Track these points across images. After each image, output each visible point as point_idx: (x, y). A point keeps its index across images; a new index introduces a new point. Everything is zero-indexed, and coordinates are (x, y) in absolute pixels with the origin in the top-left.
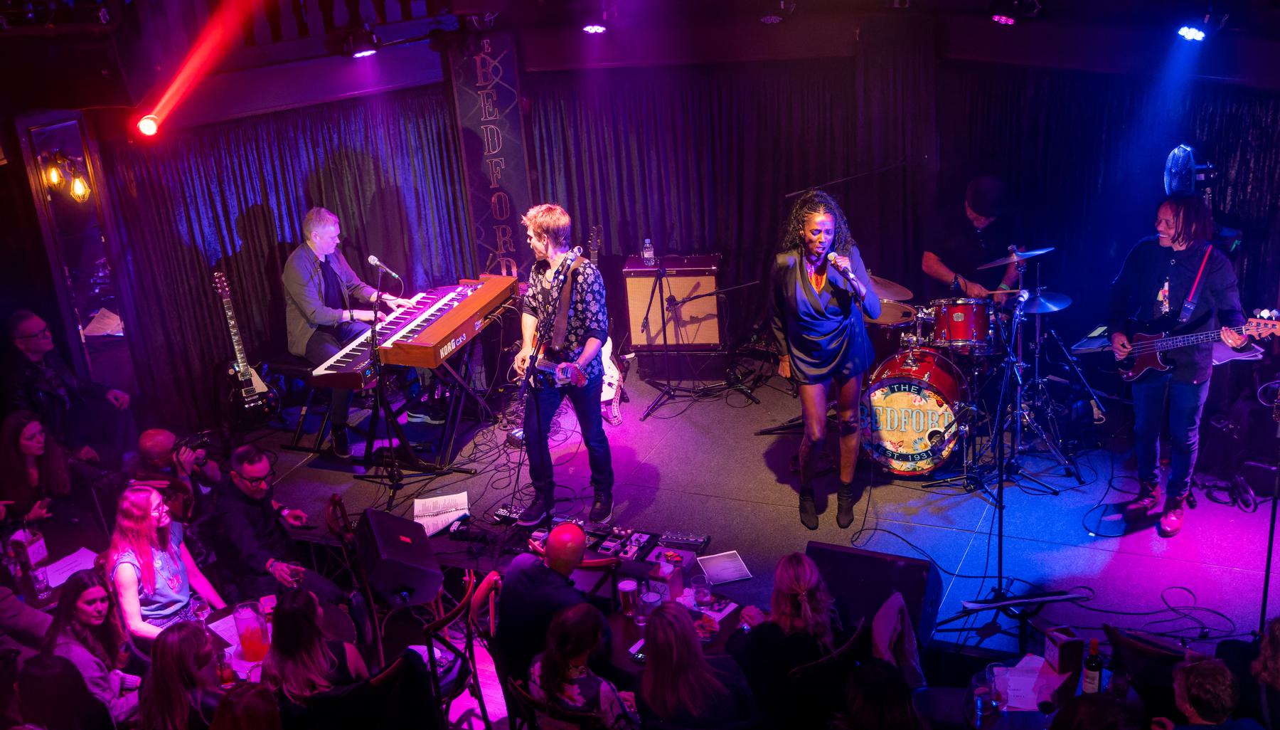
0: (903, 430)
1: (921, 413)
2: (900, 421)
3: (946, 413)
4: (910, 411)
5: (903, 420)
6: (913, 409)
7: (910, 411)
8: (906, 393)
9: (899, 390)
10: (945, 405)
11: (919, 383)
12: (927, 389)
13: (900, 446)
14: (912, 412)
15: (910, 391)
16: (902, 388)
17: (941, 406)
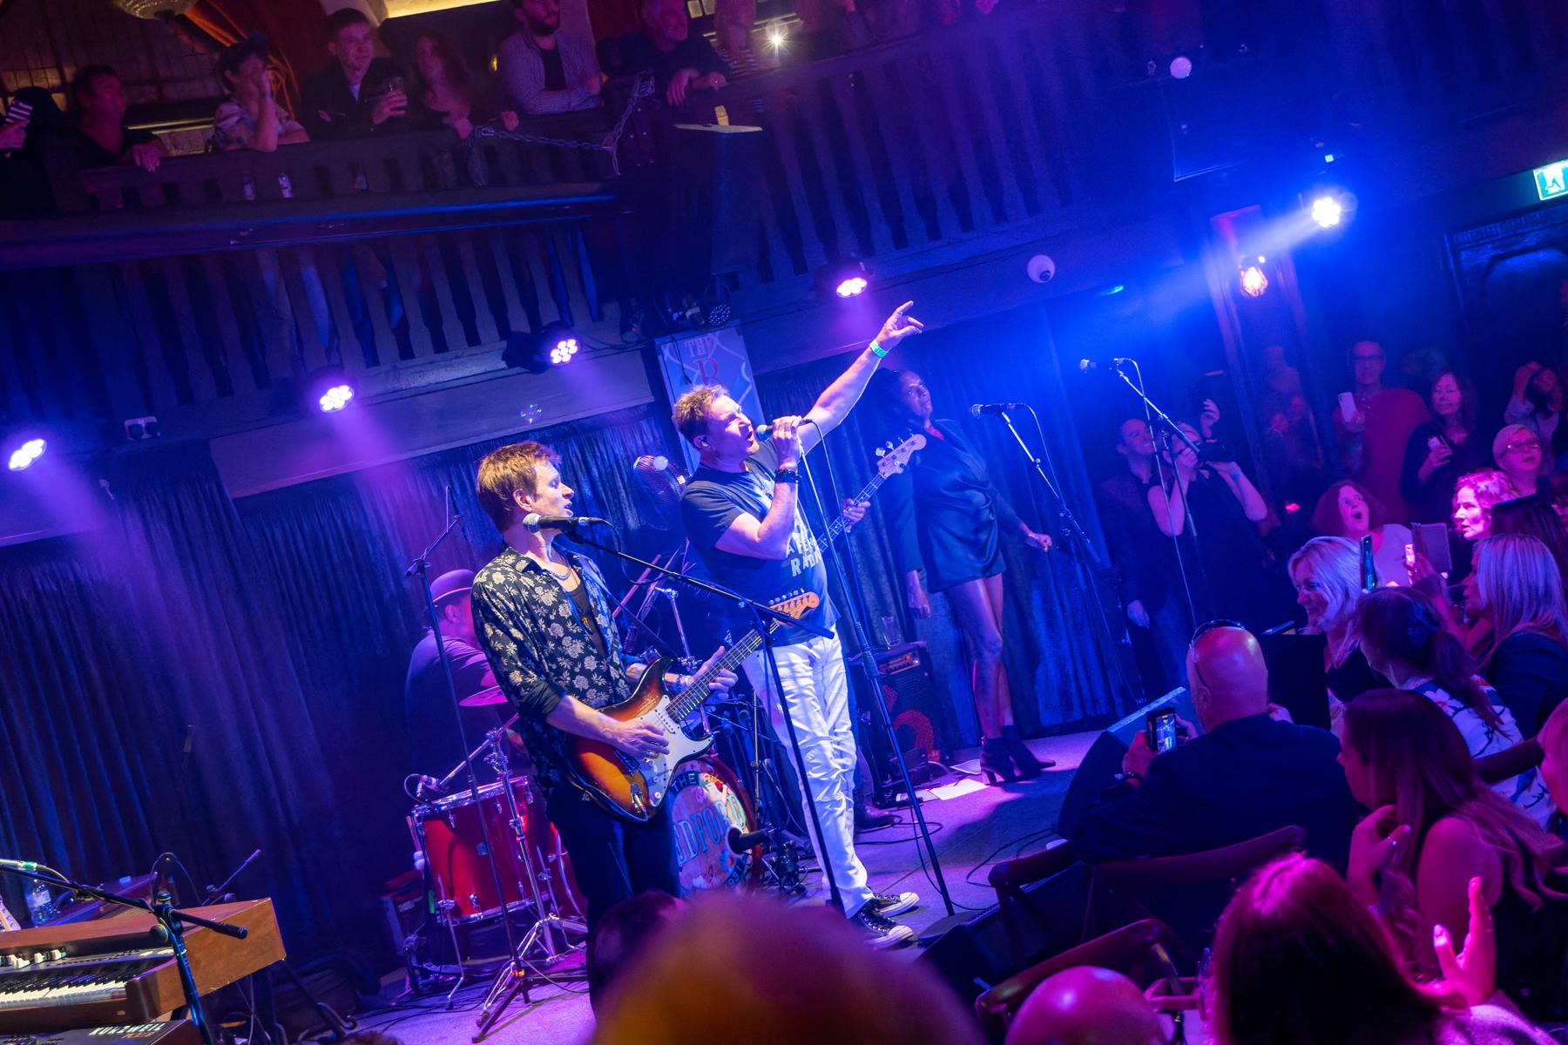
0: (705, 849)
1: (711, 812)
2: (696, 835)
3: (729, 798)
4: (699, 814)
5: (699, 832)
6: (701, 809)
7: (699, 814)
8: (685, 789)
9: (680, 789)
10: (724, 786)
11: (692, 766)
12: (702, 772)
13: (712, 876)
14: (702, 813)
15: (689, 784)
16: (681, 782)
17: (721, 790)
